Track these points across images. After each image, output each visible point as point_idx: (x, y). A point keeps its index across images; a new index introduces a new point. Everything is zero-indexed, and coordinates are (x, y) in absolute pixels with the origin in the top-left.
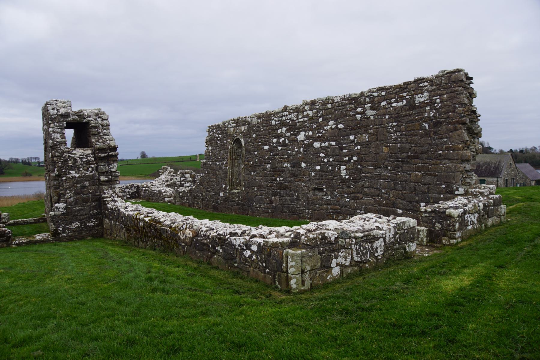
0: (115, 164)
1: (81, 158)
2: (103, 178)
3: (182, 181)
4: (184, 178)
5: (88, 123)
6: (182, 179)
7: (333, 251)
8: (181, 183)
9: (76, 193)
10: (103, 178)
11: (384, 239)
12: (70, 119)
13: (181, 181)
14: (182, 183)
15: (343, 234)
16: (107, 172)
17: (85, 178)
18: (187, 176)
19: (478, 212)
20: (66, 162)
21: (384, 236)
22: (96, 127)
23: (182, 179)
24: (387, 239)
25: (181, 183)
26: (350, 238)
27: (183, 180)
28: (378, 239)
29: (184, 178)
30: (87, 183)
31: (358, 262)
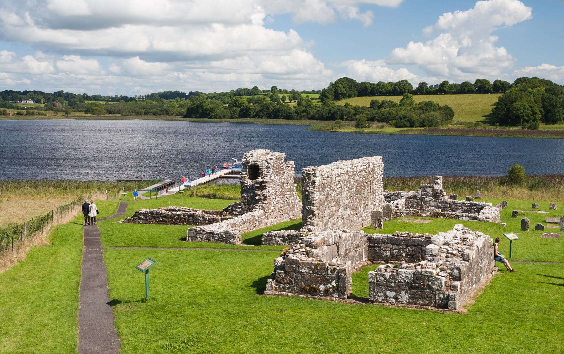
3: (423, 195)
4: (425, 192)
6: (423, 192)
8: (422, 197)
12: (249, 164)
13: (422, 195)
14: (423, 196)
18: (428, 190)
23: (423, 192)
25: (422, 197)
26: (205, 231)
27: (424, 194)
29: (425, 192)
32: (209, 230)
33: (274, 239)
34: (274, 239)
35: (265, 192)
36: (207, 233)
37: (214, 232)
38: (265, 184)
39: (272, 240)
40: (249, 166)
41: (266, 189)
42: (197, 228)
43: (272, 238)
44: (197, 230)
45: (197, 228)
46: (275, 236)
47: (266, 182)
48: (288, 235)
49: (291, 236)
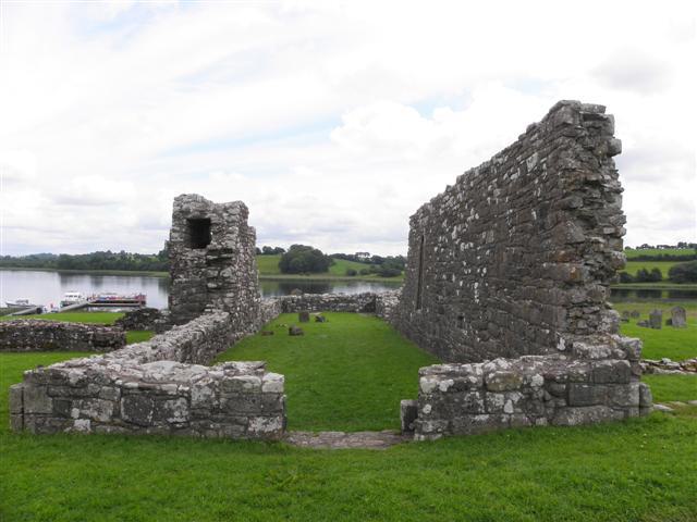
0: (229, 269)
1: (192, 261)
2: (211, 285)
5: (209, 220)
7: (77, 397)
9: (183, 301)
10: (211, 285)
11: (189, 399)
12: (190, 216)
15: (93, 377)
16: (217, 278)
17: (190, 284)
19: (526, 388)
20: (177, 265)
21: (186, 395)
22: (217, 224)
24: (194, 399)
28: (176, 397)
30: (194, 290)
31: (127, 421)
32: (135, 379)
33: (481, 402)
34: (481, 402)
35: (227, 272)
36: (125, 391)
37: (164, 387)
38: (229, 256)
39: (473, 409)
40: (188, 220)
41: (229, 265)
42: (72, 371)
43: (473, 398)
44: (72, 381)
45: (72, 371)
46: (485, 387)
47: (229, 251)
48: (549, 380)
49: (568, 382)
